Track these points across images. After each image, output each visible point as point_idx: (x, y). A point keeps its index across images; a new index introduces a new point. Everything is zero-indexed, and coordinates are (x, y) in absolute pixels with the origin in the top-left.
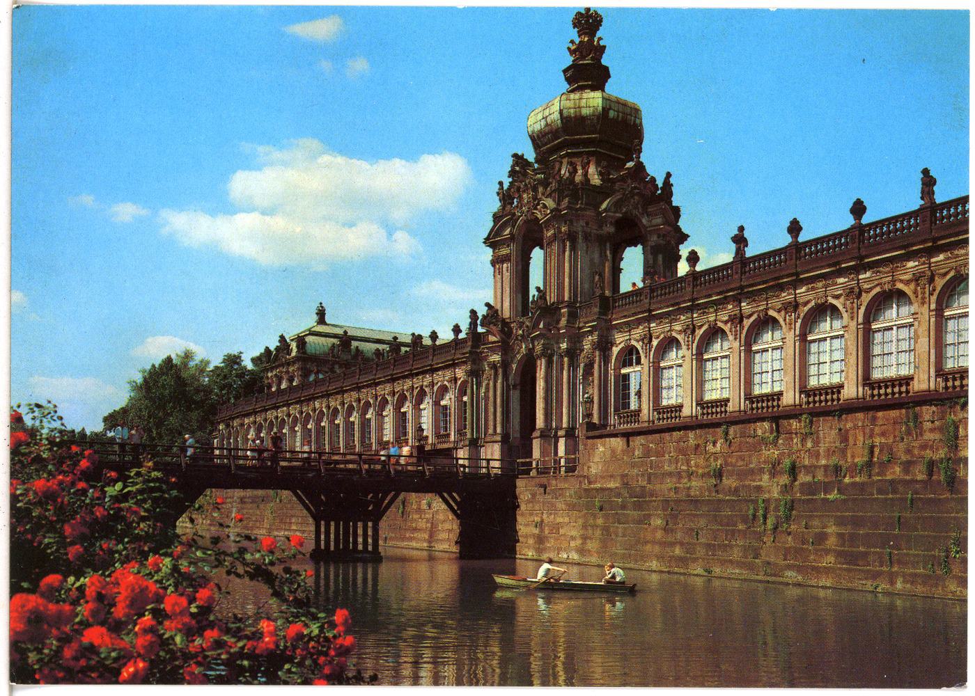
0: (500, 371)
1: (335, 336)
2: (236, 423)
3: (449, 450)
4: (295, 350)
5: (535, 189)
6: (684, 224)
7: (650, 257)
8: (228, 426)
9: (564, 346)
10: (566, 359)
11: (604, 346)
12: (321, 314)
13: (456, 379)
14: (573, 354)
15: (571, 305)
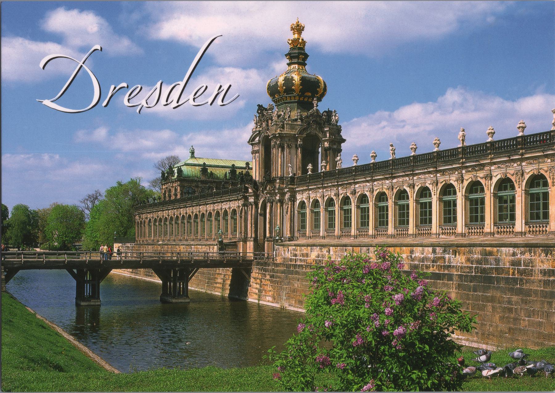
0: (254, 206)
1: (199, 165)
2: (144, 216)
3: (235, 242)
4: (176, 174)
5: (268, 122)
6: (343, 134)
7: (324, 152)
8: (140, 217)
9: (278, 198)
10: (279, 204)
11: (293, 199)
12: (193, 153)
13: (239, 207)
14: (281, 202)
15: (281, 178)
